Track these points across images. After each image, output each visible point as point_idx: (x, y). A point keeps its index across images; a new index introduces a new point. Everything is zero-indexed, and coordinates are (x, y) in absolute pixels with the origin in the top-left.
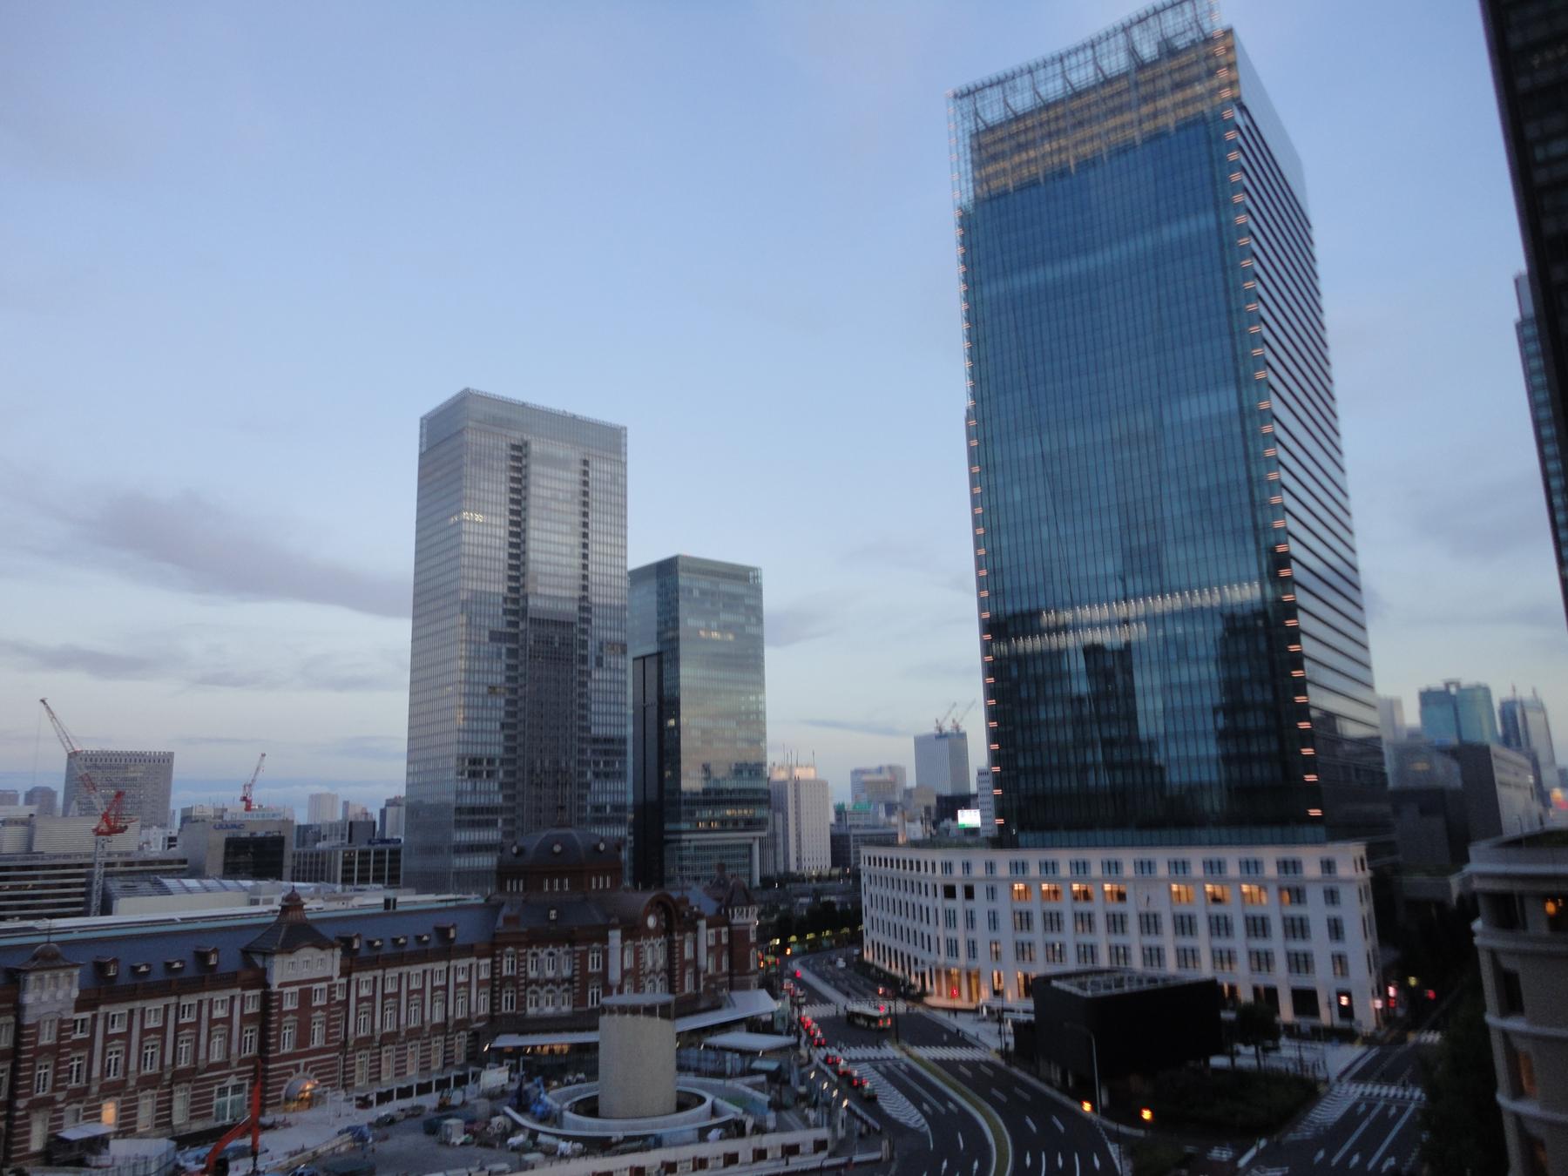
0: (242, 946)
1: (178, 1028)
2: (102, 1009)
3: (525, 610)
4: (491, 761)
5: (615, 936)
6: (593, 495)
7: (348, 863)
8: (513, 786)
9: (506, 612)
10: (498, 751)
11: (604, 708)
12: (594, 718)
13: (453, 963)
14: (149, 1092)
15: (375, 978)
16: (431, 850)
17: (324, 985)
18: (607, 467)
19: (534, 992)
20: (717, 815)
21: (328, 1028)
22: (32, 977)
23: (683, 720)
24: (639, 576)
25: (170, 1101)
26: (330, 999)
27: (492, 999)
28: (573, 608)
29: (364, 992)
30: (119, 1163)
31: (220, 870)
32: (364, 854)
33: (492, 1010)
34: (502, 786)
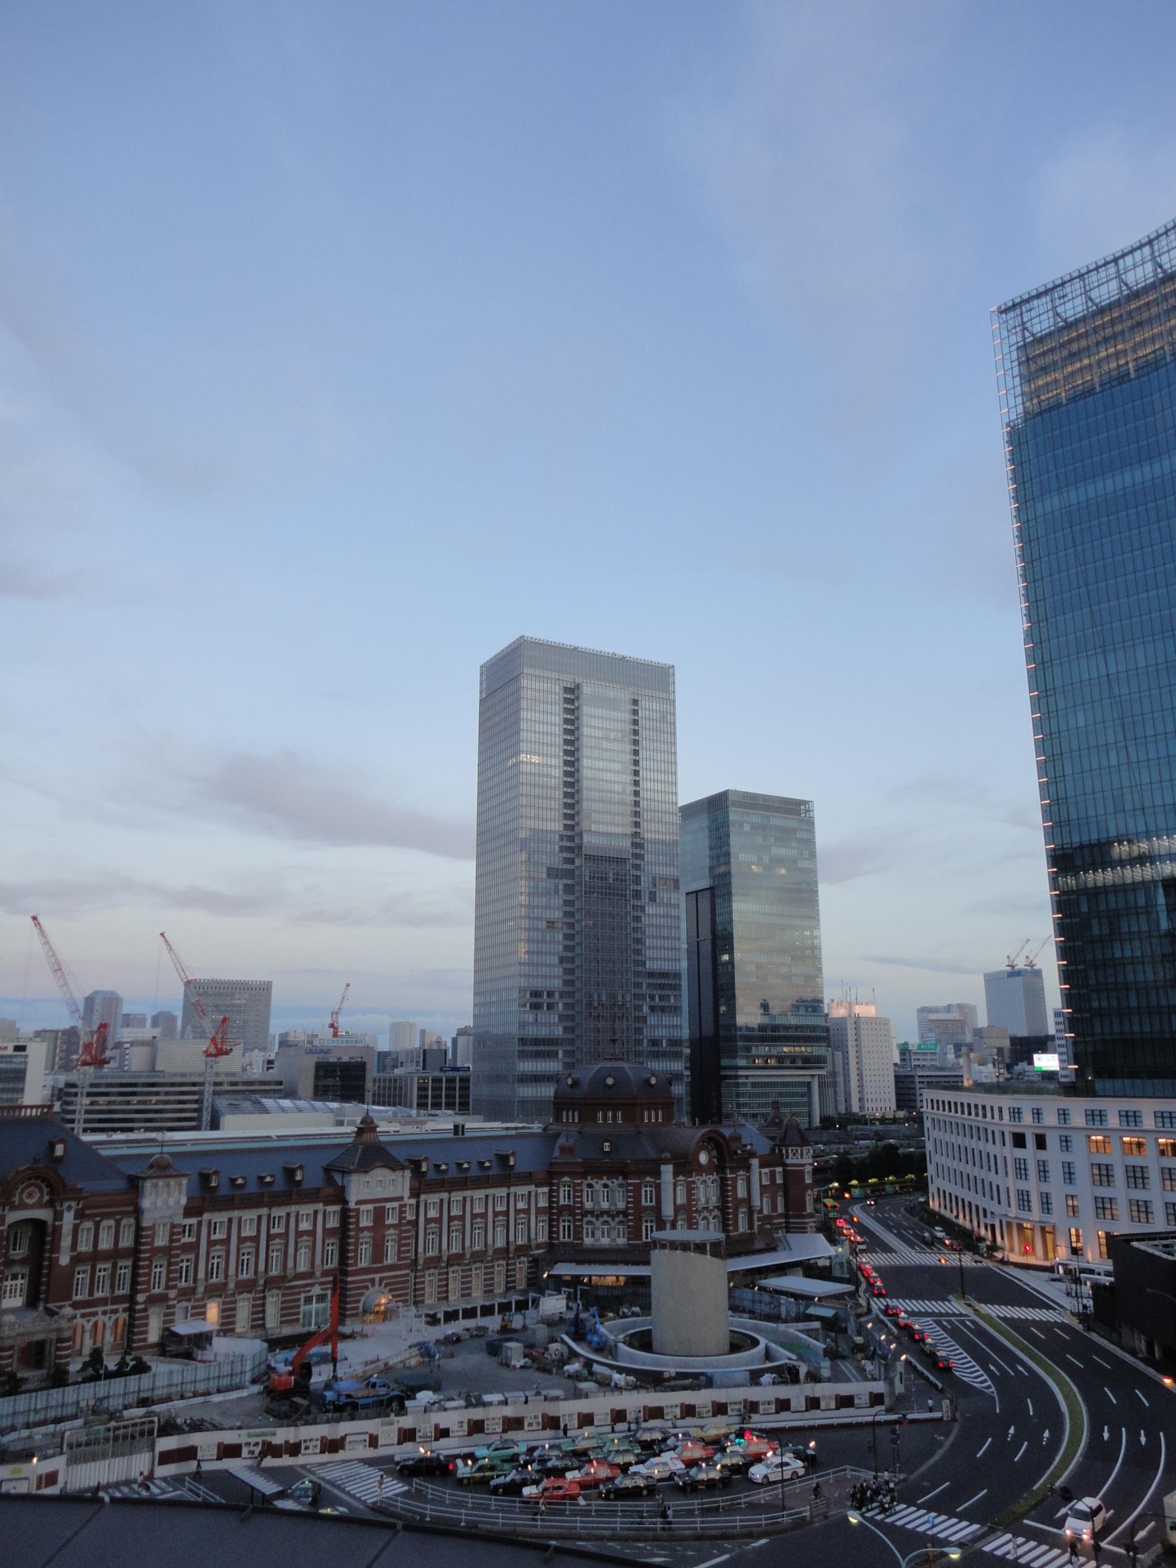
0: (325, 1163)
1: (270, 1237)
2: (206, 1216)
3: (580, 847)
4: (550, 994)
5: (667, 1170)
6: (643, 733)
7: (422, 1088)
8: (571, 1018)
9: (562, 849)
10: (557, 984)
11: (659, 943)
12: (649, 953)
13: (513, 1189)
14: (245, 1295)
15: (442, 1201)
16: (497, 1078)
17: (396, 1204)
19: (589, 1223)
20: (774, 1052)
21: (400, 1246)
23: (737, 955)
24: (689, 811)
25: (263, 1305)
26: (401, 1218)
27: (551, 1226)
28: (626, 844)
29: (432, 1214)
30: (220, 1359)
31: (310, 1092)
32: (437, 1080)
33: (550, 1238)
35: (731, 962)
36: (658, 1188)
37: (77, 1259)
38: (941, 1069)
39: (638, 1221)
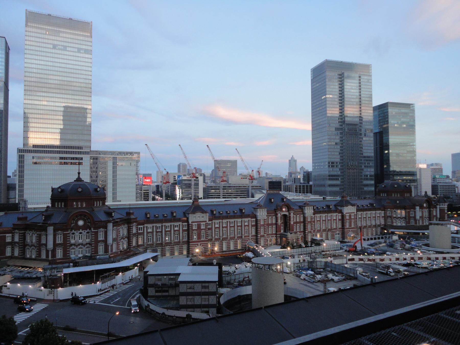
3: (344, 121)
4: (337, 163)
5: (418, 208)
8: (343, 169)
9: (339, 122)
10: (338, 160)
11: (367, 148)
12: (364, 151)
18: (366, 77)
20: (401, 178)
22: (306, 208)
23: (390, 151)
24: (375, 109)
28: (357, 120)
29: (360, 217)
32: (300, 186)
34: (340, 169)
35: (388, 153)
36: (415, 212)
37: (294, 223)
38: (446, 183)
39: (409, 220)
